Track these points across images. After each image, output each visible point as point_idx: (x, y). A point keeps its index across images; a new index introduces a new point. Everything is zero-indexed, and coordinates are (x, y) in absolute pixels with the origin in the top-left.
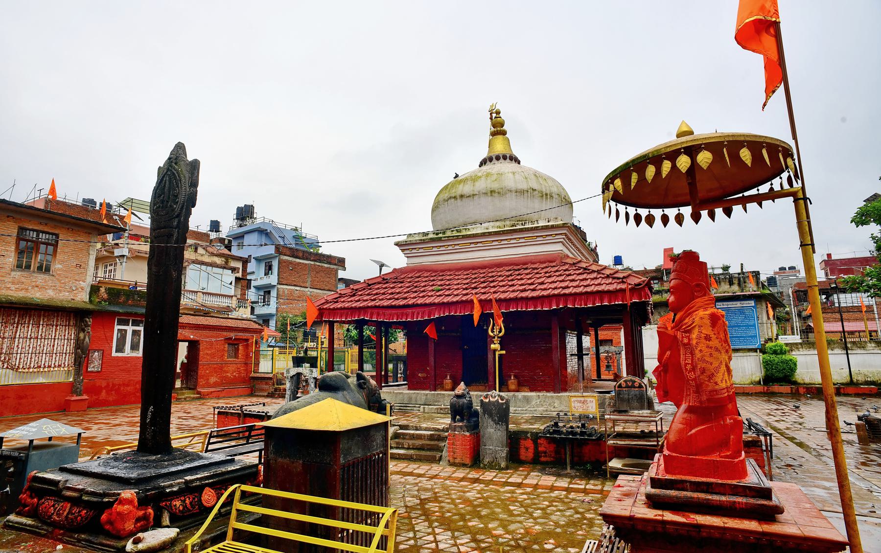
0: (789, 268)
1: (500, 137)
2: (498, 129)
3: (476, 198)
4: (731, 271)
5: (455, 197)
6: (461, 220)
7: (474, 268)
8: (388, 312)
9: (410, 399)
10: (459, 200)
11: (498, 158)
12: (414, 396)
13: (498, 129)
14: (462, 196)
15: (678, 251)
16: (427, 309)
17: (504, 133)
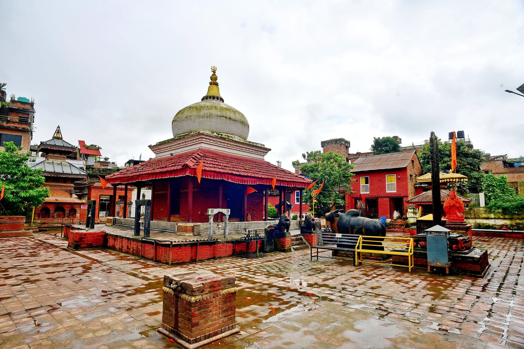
0: (112, 163)
1: (214, 86)
2: (214, 82)
3: (237, 122)
4: (109, 161)
5: (226, 117)
6: (226, 131)
7: (233, 158)
8: (236, 178)
9: (238, 226)
10: (228, 120)
11: (214, 98)
12: (240, 225)
13: (214, 82)
14: (230, 118)
15: (88, 143)
16: (253, 180)
17: (217, 84)
